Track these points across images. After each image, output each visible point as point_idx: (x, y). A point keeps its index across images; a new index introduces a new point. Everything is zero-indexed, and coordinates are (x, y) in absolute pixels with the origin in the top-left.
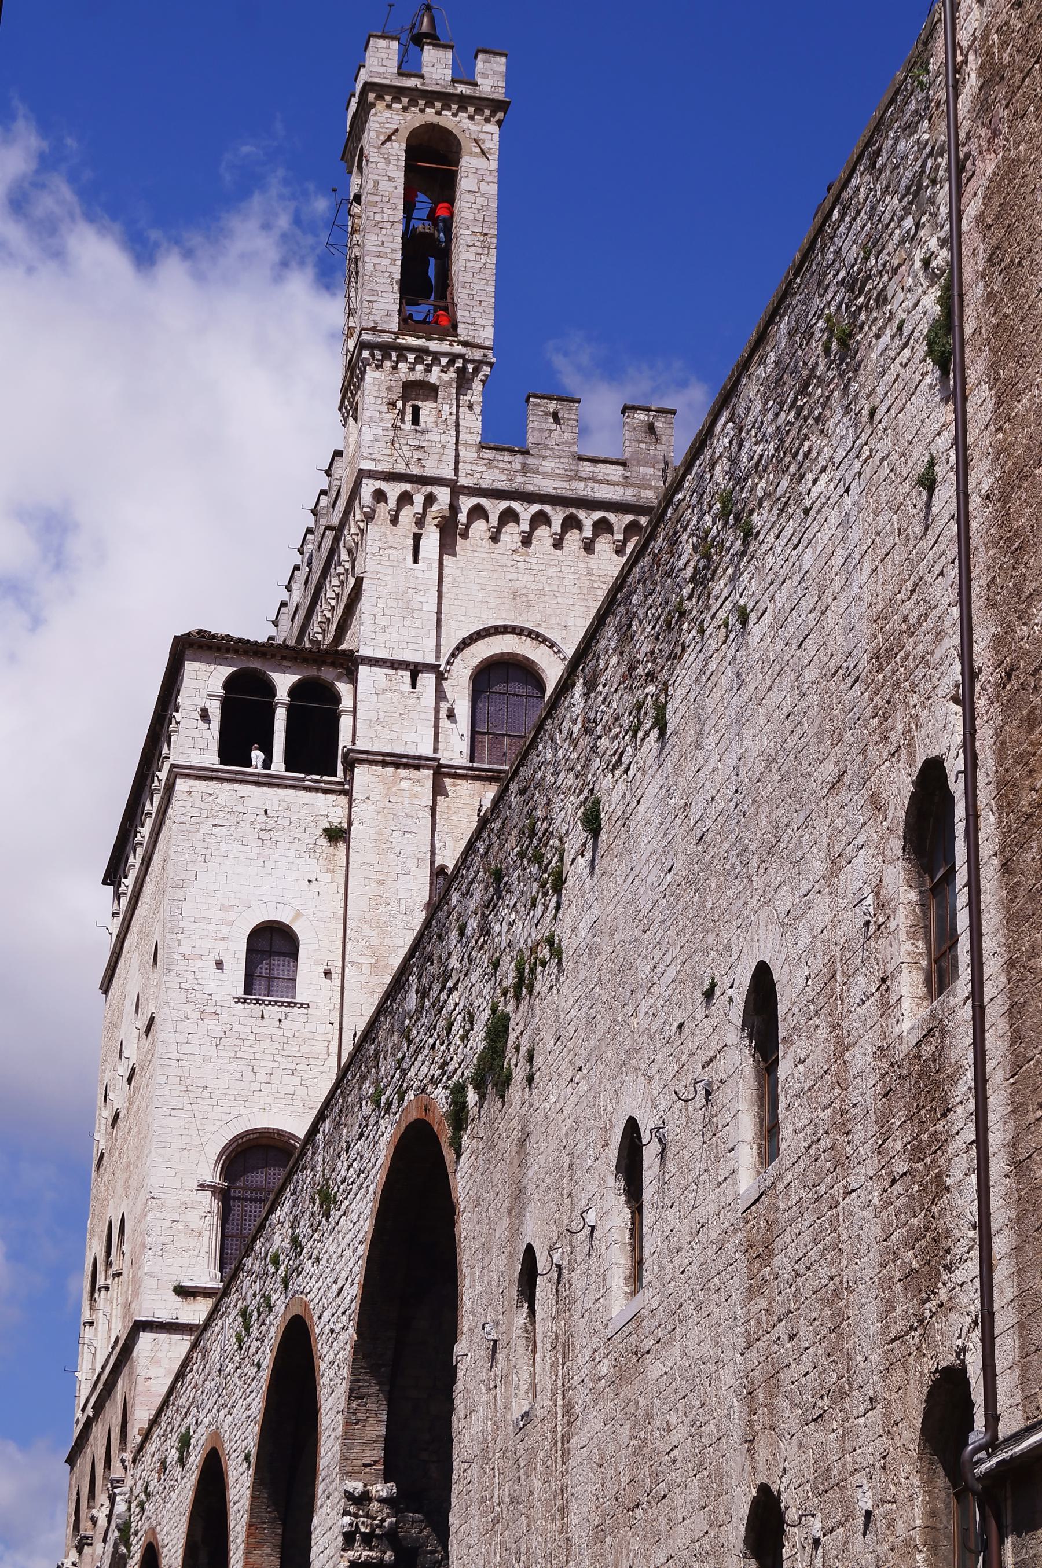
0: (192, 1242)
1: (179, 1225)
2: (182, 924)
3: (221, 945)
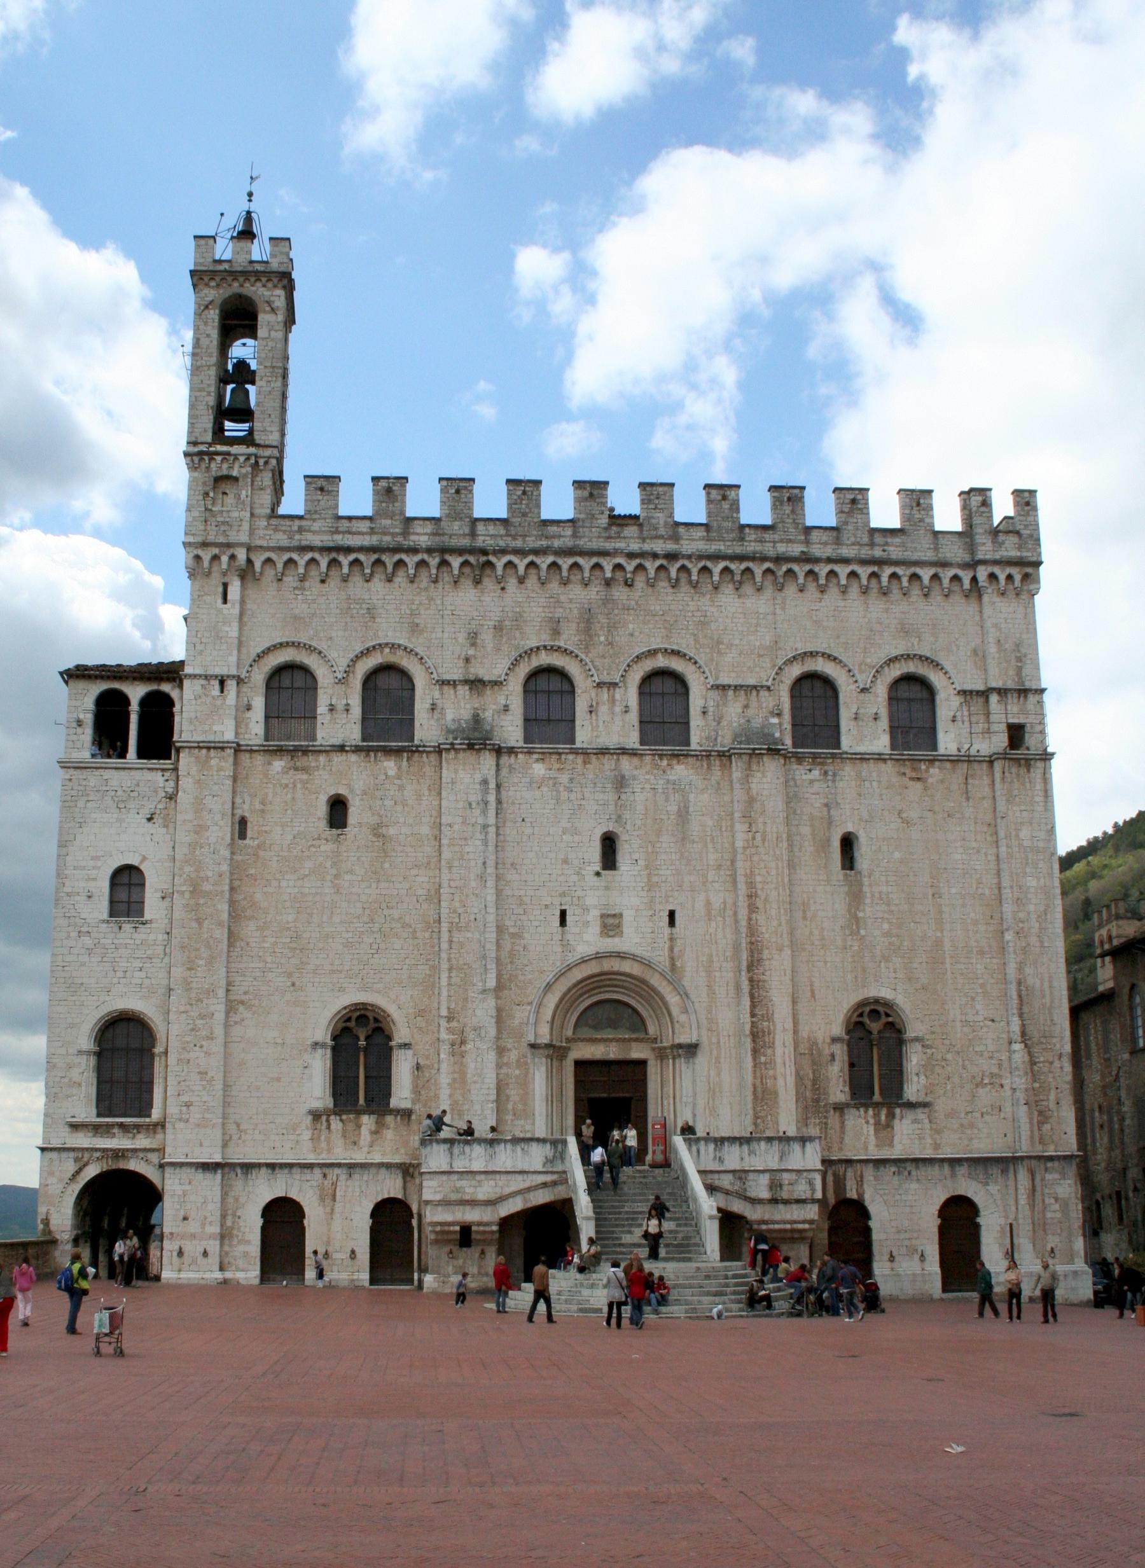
0: (75, 1091)
1: (66, 1080)
2: (66, 872)
3: (91, 884)
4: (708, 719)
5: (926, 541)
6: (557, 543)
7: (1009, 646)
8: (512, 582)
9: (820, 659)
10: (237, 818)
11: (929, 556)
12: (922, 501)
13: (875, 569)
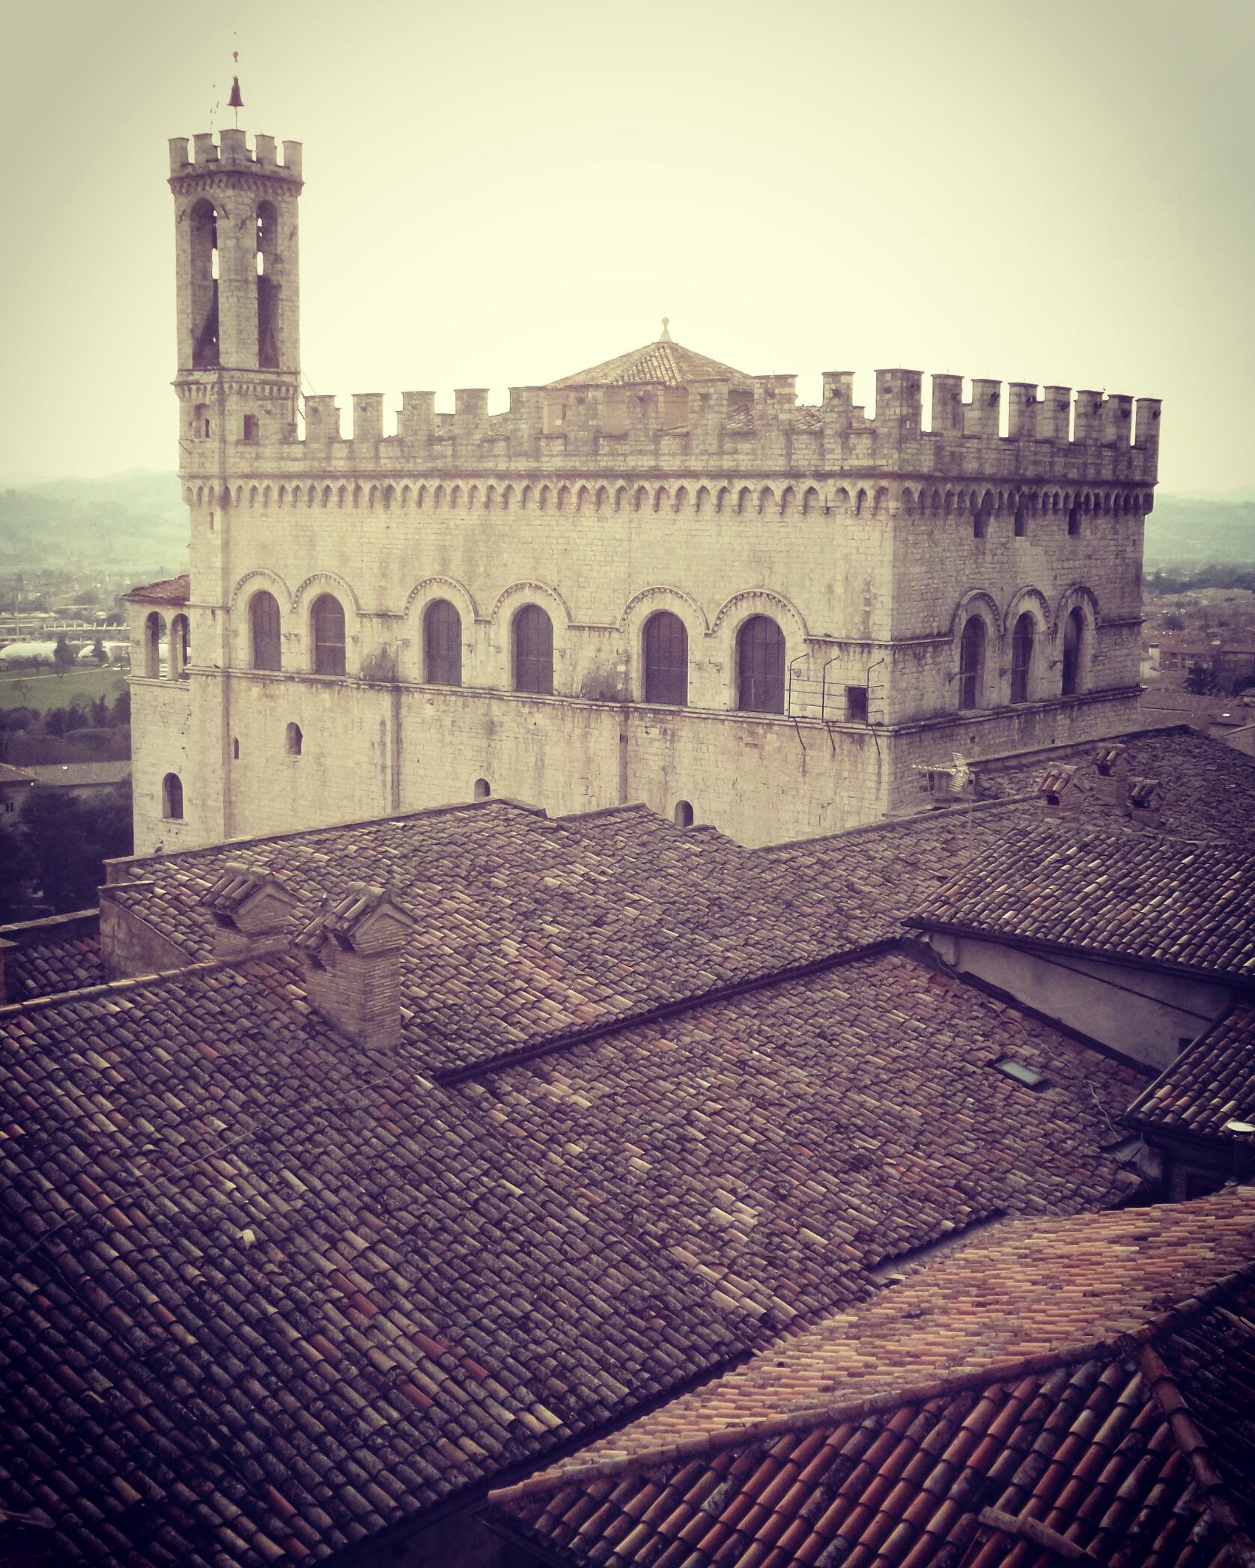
4: (572, 663)
5: (777, 444)
6: (439, 464)
7: (858, 584)
8: (412, 505)
9: (669, 596)
10: (232, 741)
11: (779, 464)
12: (777, 391)
13: (725, 483)
